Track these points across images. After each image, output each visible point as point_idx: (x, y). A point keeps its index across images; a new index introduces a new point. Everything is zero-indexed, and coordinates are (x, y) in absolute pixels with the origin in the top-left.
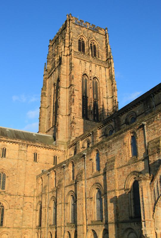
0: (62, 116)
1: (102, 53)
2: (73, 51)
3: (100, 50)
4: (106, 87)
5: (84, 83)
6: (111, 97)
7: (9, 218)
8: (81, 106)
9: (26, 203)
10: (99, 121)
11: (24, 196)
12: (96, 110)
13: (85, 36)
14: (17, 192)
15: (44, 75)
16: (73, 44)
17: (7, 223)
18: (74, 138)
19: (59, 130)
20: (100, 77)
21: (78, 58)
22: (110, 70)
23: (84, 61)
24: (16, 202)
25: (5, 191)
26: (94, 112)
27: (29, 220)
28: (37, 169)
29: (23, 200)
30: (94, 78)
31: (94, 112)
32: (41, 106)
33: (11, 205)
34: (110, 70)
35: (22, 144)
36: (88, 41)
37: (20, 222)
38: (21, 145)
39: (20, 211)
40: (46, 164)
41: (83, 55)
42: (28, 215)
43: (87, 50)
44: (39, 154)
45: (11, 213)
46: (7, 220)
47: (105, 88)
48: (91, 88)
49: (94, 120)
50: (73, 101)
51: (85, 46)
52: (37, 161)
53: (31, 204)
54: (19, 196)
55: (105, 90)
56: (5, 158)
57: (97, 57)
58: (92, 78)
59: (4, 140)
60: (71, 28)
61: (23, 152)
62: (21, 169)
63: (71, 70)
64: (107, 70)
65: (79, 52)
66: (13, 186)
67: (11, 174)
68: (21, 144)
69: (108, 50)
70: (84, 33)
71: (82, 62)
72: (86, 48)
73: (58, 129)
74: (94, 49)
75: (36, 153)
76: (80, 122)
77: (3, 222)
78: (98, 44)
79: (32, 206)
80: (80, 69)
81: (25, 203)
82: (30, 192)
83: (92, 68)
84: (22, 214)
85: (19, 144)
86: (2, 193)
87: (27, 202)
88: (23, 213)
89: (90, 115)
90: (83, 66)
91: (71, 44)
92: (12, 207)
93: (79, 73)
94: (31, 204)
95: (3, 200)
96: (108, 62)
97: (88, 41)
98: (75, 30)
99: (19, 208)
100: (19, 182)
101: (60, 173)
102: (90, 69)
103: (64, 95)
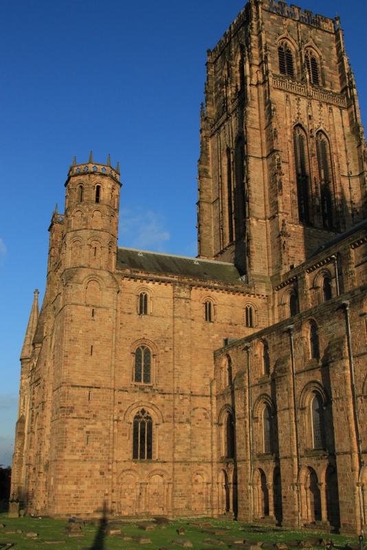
0: (257, 219)
1: (330, 75)
2: (270, 74)
4: (346, 151)
5: (298, 144)
6: (358, 173)
7: (164, 443)
8: (295, 198)
10: (334, 228)
11: (192, 395)
12: (326, 205)
13: (290, 39)
14: (176, 386)
15: (201, 131)
16: (269, 59)
17: (162, 453)
18: (286, 269)
19: (253, 252)
20: (331, 129)
21: (281, 90)
22: (352, 113)
23: (296, 94)
24: (176, 409)
25: (152, 386)
26: (323, 208)
27: (204, 445)
29: (189, 403)
30: (317, 134)
31: (323, 208)
32: (200, 198)
33: (166, 413)
34: (352, 113)
35: (181, 284)
36: (300, 49)
38: (177, 287)
39: (185, 427)
40: (231, 326)
41: (291, 81)
42: (201, 435)
43: (298, 70)
44: (214, 305)
45: (167, 432)
46: (159, 447)
47: (343, 154)
48: (313, 155)
49: (325, 227)
50: (281, 187)
51: (294, 60)
52: (212, 320)
53: (205, 412)
55: (343, 159)
56: (146, 316)
57: (321, 85)
58: (314, 134)
59: (143, 277)
60: (261, 22)
61: (183, 301)
62: (181, 338)
63: (271, 117)
64: (346, 113)
65: (281, 75)
66: (167, 374)
68: (178, 284)
69: (344, 69)
70: (289, 32)
71: (292, 97)
72: (296, 64)
73: (251, 250)
74: (313, 65)
75: (208, 303)
76: (294, 232)
77: (153, 450)
78: (320, 54)
80: (288, 113)
81: (194, 409)
82: (202, 385)
83: (313, 110)
84: (189, 433)
85: (174, 283)
86: (146, 390)
87: (197, 408)
88: (191, 430)
89: (315, 217)
90: (294, 108)
91: (266, 57)
92: (169, 419)
94: (205, 412)
95: (150, 405)
96: (347, 94)
97: (298, 48)
98: (270, 25)
99: (183, 421)
100: (180, 365)
101: (279, 344)
102: (309, 114)
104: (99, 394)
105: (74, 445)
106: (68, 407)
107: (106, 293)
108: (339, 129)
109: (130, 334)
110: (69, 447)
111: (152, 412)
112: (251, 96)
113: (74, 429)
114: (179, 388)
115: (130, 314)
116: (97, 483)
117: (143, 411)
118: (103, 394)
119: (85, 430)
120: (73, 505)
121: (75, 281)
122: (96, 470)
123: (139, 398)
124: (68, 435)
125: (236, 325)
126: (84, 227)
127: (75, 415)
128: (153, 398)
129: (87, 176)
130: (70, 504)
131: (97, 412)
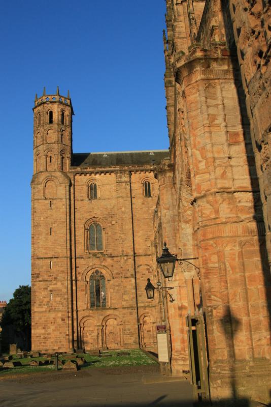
7: (115, 294)
9: (140, 267)
14: (121, 250)
15: (164, 52)
17: (113, 301)
32: (168, 104)
33: (115, 271)
35: (121, 172)
37: (133, 298)
38: (118, 175)
39: (130, 281)
44: (152, 183)
45: (117, 286)
46: (111, 297)
52: (152, 195)
53: (148, 267)
54: (125, 256)
56: (95, 200)
62: (124, 213)
66: (114, 242)
67: (108, 223)
68: (119, 172)
75: (147, 183)
79: (151, 270)
81: (138, 267)
82: (145, 247)
85: (116, 172)
86: (98, 256)
87: (141, 265)
92: (117, 276)
94: (148, 267)
95: (101, 266)
99: (128, 276)
100: (123, 234)
104: (58, 262)
105: (41, 301)
106: (36, 274)
107: (59, 188)
109: (83, 215)
110: (38, 302)
111: (104, 272)
113: (40, 289)
114: (123, 251)
115: (82, 200)
116: (60, 327)
117: (97, 272)
118: (61, 262)
119: (49, 289)
120: (42, 344)
121: (36, 183)
122: (59, 317)
123: (93, 262)
124: (37, 294)
126: (42, 143)
127: (41, 279)
128: (104, 261)
129: (42, 106)
130: (40, 343)
131: (57, 275)
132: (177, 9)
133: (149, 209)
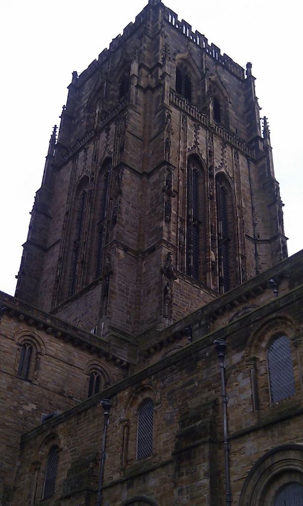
0: (126, 249)
3: (232, 112)
4: (253, 209)
6: (268, 238)
19: (113, 292)
23: (193, 119)
28: (24, 407)
44: (38, 353)
47: (249, 211)
51: (193, 88)
72: (196, 93)
73: (111, 288)
91: (164, 60)
93: (178, 144)
97: (200, 77)
101: (184, 386)
103: (133, 190)
108: (244, 180)
112: (137, 99)
125: (70, 398)
132: (137, 93)
133: (16, 409)
